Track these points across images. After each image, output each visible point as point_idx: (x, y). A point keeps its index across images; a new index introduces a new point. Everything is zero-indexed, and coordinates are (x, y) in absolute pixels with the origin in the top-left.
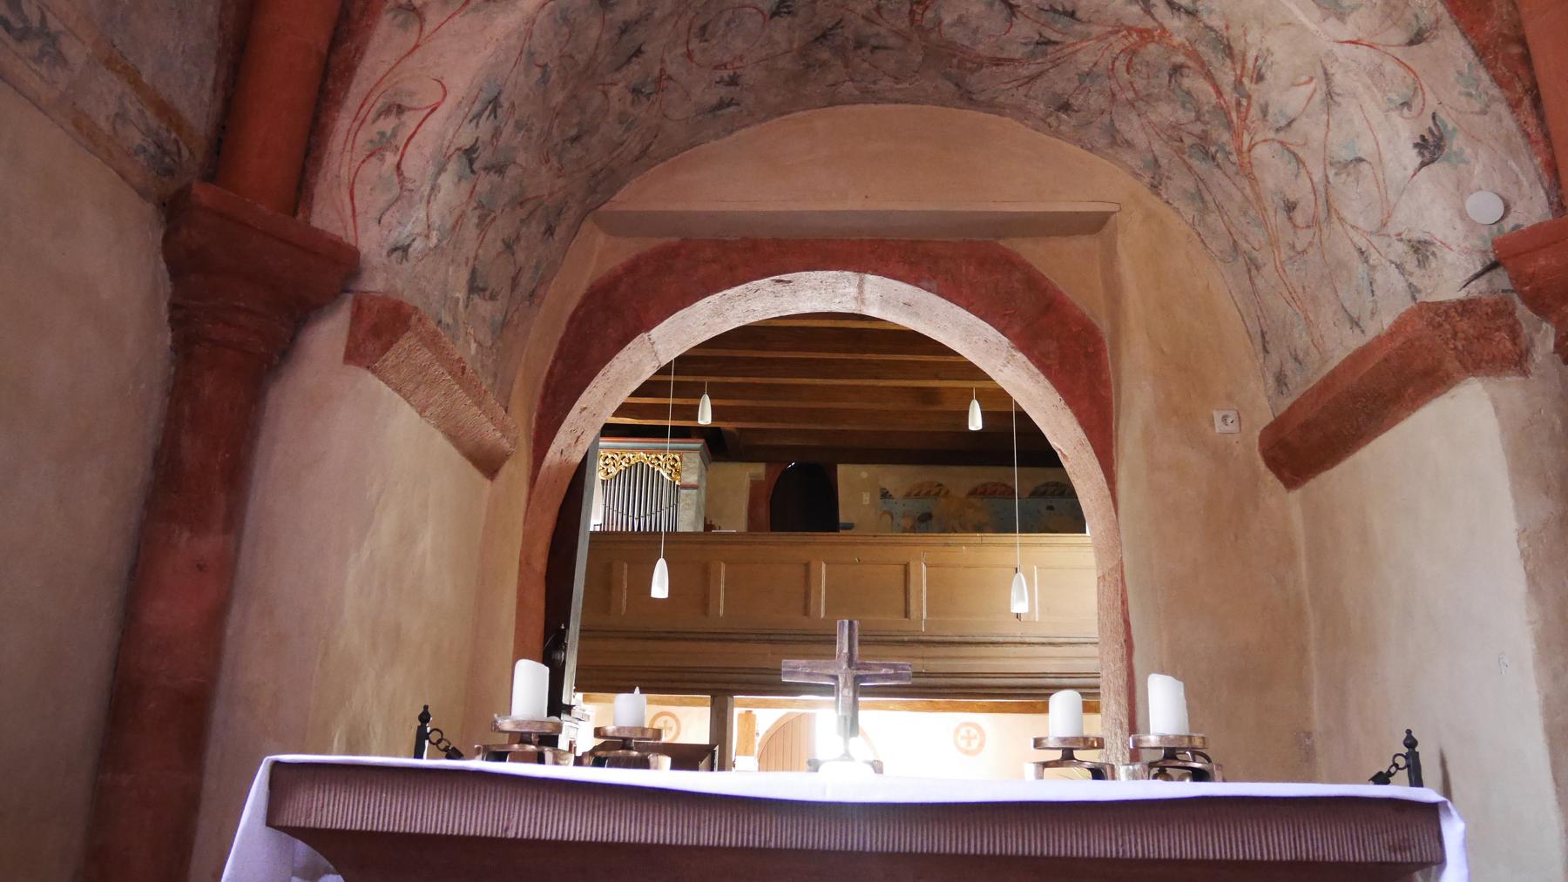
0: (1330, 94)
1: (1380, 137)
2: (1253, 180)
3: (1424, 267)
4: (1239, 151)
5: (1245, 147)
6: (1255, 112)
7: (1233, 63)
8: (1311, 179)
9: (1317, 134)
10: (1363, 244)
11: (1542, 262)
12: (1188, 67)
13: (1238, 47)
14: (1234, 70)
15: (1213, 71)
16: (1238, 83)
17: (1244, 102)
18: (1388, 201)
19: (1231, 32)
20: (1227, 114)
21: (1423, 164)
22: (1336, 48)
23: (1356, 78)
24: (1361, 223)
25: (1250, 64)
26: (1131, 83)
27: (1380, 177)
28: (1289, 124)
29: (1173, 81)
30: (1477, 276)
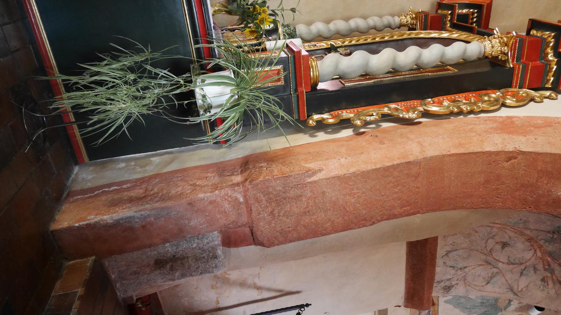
2: (530, 240)
4: (540, 247)
5: (538, 251)
6: (540, 266)
7: (558, 279)
9: (509, 276)
14: (556, 277)
16: (552, 272)
17: (547, 267)
18: (469, 286)
20: (553, 258)
25: (550, 282)
27: (476, 288)
28: (522, 273)
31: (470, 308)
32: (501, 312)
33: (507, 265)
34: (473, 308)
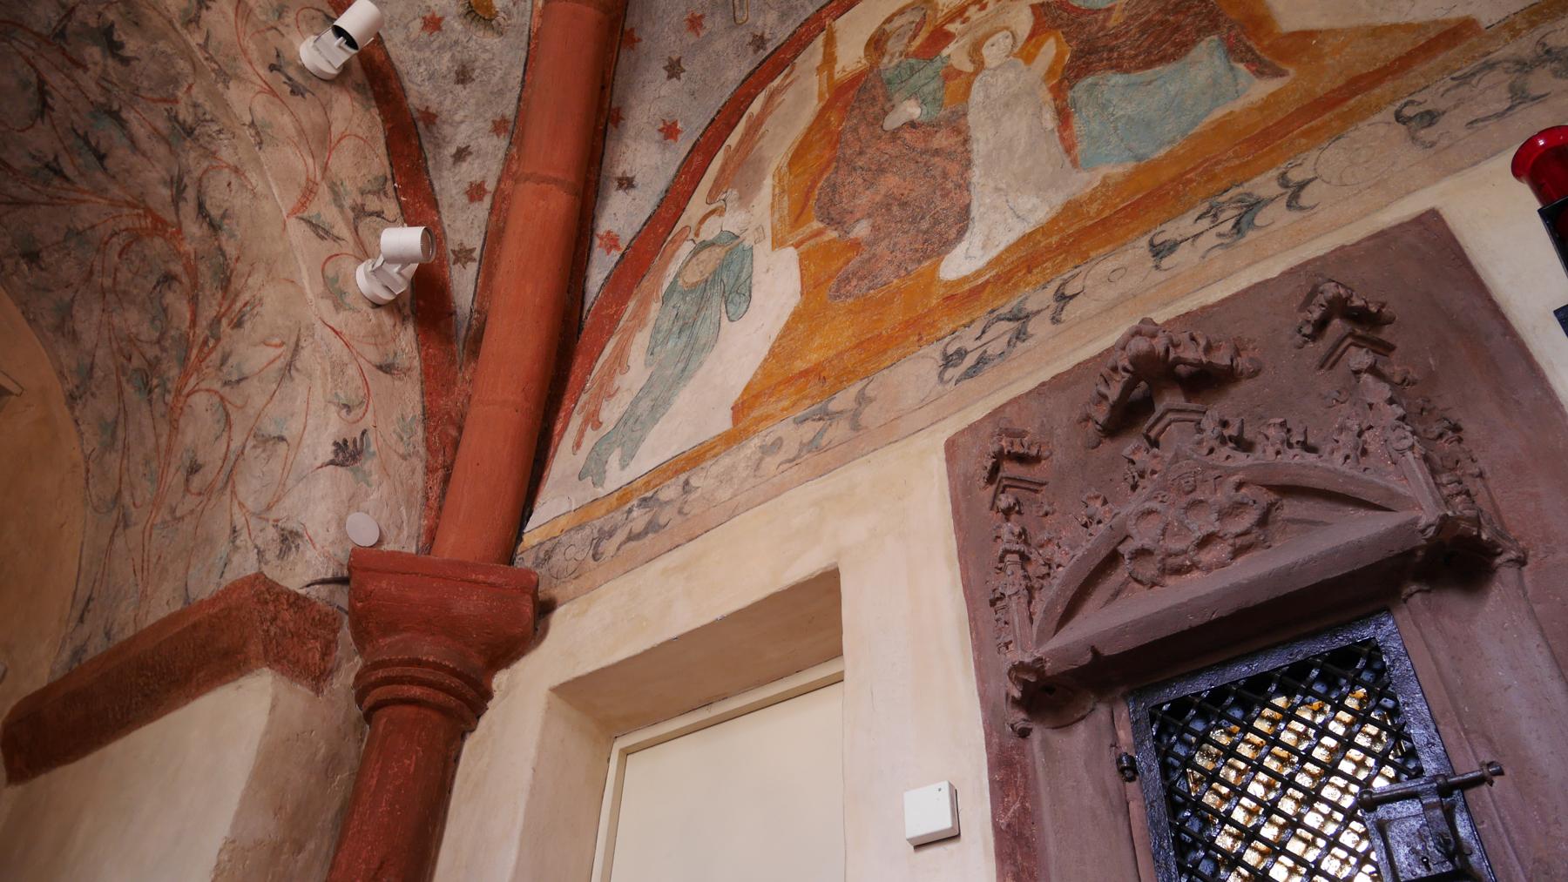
0: (290, 365)
1: (311, 421)
2: (174, 427)
4: (179, 392)
5: (185, 391)
6: (215, 357)
7: (223, 297)
8: (228, 446)
9: (258, 401)
10: (239, 521)
11: (384, 585)
12: (181, 283)
13: (236, 284)
14: (220, 305)
15: (200, 298)
16: (217, 321)
17: (211, 343)
19: (239, 265)
20: (189, 349)
21: (332, 463)
22: (319, 325)
23: (319, 360)
24: (250, 504)
25: (239, 305)
26: (116, 270)
28: (239, 381)
29: (158, 289)
30: (323, 582)
33: (233, 429)
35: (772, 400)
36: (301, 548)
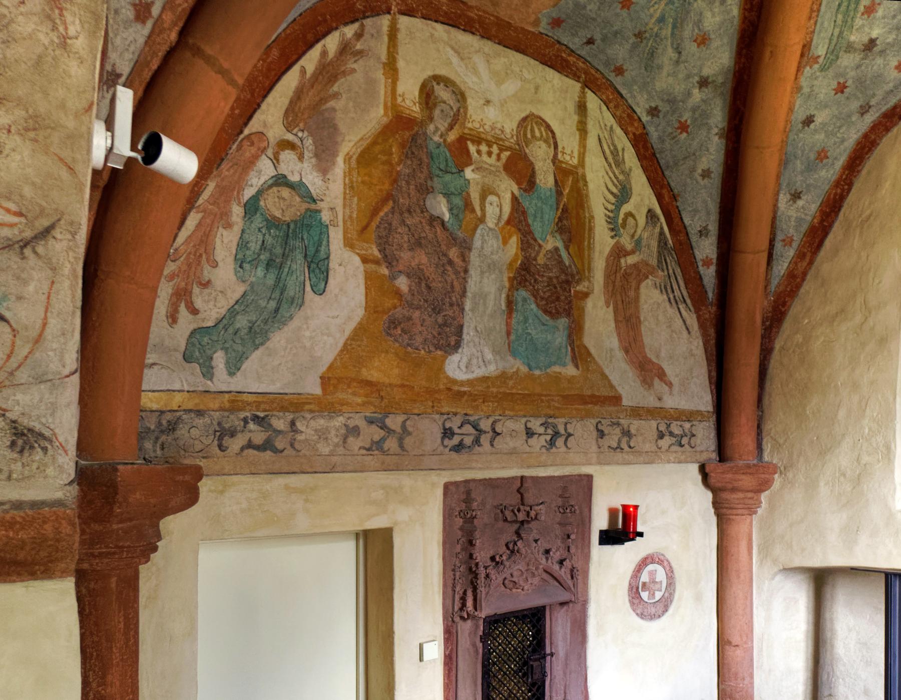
3: (21, 452)
31: (280, 302)
32: (319, 211)
34: (282, 294)
35: (350, 391)
36: (50, 452)
